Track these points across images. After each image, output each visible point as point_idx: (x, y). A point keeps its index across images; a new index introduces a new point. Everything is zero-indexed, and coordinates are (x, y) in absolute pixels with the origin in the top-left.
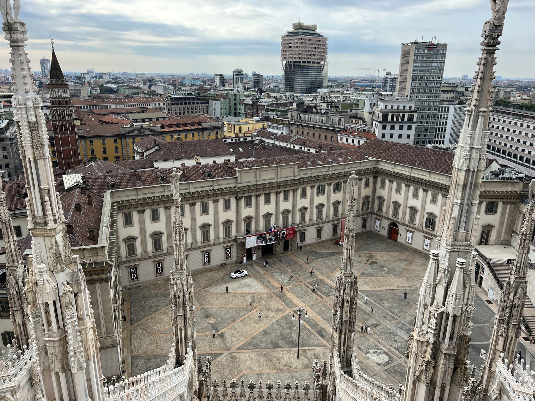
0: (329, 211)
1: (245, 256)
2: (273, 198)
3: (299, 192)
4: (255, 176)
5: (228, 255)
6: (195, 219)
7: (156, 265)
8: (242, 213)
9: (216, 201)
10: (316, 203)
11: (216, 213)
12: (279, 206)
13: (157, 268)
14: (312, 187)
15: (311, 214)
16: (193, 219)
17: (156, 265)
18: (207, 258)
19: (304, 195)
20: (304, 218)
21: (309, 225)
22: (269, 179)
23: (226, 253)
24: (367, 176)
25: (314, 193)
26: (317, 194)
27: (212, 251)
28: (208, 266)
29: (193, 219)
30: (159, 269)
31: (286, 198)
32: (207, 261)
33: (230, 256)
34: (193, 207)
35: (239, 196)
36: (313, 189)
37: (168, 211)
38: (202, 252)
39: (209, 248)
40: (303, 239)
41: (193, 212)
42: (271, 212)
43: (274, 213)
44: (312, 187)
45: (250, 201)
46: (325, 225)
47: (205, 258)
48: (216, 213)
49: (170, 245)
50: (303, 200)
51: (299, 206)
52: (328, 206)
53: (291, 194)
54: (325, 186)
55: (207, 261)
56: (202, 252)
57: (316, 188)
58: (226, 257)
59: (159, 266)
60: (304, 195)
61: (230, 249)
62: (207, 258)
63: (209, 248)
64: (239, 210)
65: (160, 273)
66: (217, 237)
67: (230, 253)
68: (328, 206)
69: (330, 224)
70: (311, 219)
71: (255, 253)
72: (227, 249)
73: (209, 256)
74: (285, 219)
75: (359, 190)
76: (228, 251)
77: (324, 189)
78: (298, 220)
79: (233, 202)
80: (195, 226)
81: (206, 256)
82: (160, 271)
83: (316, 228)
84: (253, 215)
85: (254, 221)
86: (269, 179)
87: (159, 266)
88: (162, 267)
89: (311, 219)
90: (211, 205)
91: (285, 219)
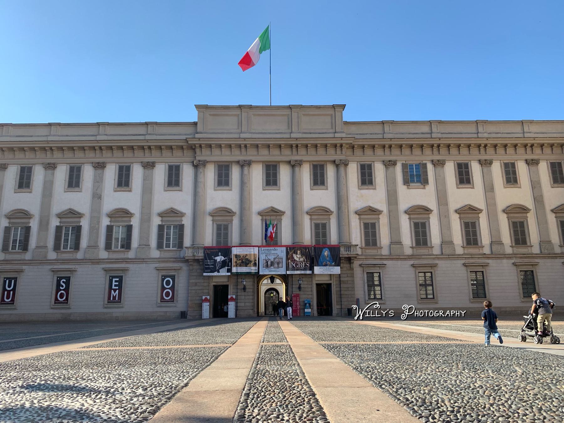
0: (449, 228)
1: (206, 300)
2: (284, 173)
4: (238, 126)
5: (168, 294)
6: (100, 197)
7: (5, 282)
8: (208, 201)
9: (149, 166)
11: (147, 190)
13: (4, 289)
15: (394, 228)
16: (97, 196)
17: (5, 282)
18: (115, 290)
21: (391, 257)
22: (270, 133)
23: (163, 288)
26: (406, 182)
28: (116, 311)
29: (97, 196)
30: (9, 292)
32: (114, 298)
34: (99, 171)
35: (198, 158)
36: (391, 169)
37: (50, 172)
41: (98, 181)
43: (288, 213)
44: (389, 164)
45: (227, 176)
46: (442, 264)
47: (110, 288)
48: (147, 190)
49: (42, 244)
50: (367, 192)
52: (444, 218)
54: (425, 166)
55: (114, 298)
57: (399, 168)
58: (162, 298)
59: (9, 287)
61: (173, 277)
62: (115, 290)
64: (200, 190)
65: (8, 303)
66: (145, 245)
67: (173, 288)
68: (444, 218)
71: (232, 299)
72: (165, 277)
73: (120, 286)
75: (533, 188)
76: (168, 283)
77: (426, 173)
79: (187, 172)
80: (99, 212)
81: (114, 283)
82: (8, 298)
83: (413, 266)
84: (234, 207)
85: (236, 221)
86: (270, 133)
87: (9, 287)
88: (14, 290)
89: (396, 242)
90: (137, 173)
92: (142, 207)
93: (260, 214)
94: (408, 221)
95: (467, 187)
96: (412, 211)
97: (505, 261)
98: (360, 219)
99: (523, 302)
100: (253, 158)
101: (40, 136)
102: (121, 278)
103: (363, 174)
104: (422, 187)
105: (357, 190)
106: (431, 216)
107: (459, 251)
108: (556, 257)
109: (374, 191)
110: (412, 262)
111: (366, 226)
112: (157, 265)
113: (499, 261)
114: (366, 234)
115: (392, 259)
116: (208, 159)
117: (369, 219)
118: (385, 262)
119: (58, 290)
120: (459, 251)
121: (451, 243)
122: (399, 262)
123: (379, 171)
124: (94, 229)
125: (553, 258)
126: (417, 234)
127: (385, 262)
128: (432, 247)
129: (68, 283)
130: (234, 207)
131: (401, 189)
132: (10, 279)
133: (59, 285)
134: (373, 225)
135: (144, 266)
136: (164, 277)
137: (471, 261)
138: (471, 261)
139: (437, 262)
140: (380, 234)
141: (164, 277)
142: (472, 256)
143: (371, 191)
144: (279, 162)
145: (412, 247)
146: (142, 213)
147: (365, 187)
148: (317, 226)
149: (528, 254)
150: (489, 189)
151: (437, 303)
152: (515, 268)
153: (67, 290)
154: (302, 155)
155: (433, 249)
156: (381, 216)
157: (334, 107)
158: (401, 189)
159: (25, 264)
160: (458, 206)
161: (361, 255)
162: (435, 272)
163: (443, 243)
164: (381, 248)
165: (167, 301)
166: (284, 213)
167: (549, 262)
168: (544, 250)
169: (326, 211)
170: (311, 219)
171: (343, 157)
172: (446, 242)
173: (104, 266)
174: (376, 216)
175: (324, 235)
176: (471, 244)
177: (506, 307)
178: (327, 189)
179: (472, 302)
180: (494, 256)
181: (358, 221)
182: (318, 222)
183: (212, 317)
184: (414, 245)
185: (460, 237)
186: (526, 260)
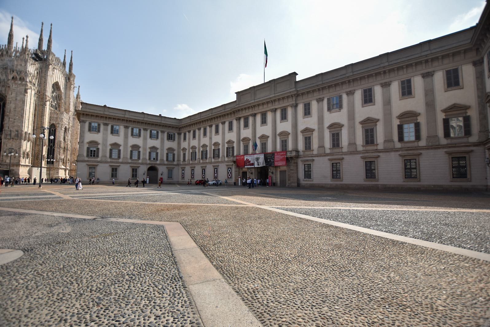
2: (269, 116)
3: (301, 108)
10: (327, 124)
12: (272, 126)
14: (320, 100)
15: (321, 138)
16: (211, 138)
19: (307, 112)
20: (310, 143)
21: (317, 156)
23: (228, 173)
24: (450, 65)
25: (322, 109)
26: (329, 109)
27: (219, 167)
29: (211, 138)
31: (284, 117)
33: (231, 177)
34: (211, 128)
35: (237, 116)
36: (321, 103)
38: (214, 166)
39: (217, 164)
40: (308, 175)
41: (211, 132)
42: (267, 134)
44: (320, 100)
48: (224, 134)
50: (308, 119)
51: (301, 127)
52: (352, 128)
53: (290, 111)
56: (214, 166)
57: (325, 102)
60: (307, 112)
63: (217, 164)
68: (352, 128)
69: (358, 157)
70: (321, 146)
74: (284, 143)
75: (426, 95)
78: (301, 146)
81: (216, 171)
83: (329, 160)
84: (250, 136)
89: (321, 146)
91: (284, 143)
92: (222, 141)
93: (259, 138)
94: (329, 133)
95: (369, 105)
96: (331, 127)
97: (393, 153)
98: (303, 135)
99: (404, 181)
100: (255, 112)
101: (198, 118)
102: (217, 169)
103: (305, 109)
104: (339, 111)
105: (302, 119)
106: (343, 128)
107: (360, 148)
108: (439, 148)
109: (311, 118)
110: (329, 157)
111: (306, 138)
112: (226, 164)
113: (388, 154)
114: (306, 143)
115: (318, 156)
116: (240, 116)
117: (307, 134)
118: (314, 158)
119: (203, 174)
120: (360, 148)
121: (355, 144)
122: (322, 158)
123: (314, 106)
124: (210, 151)
125: (435, 148)
126: (333, 140)
127: (314, 158)
128: (342, 148)
129: (204, 171)
130: (250, 137)
131: (326, 114)
132: (192, 170)
133: (203, 172)
134: (310, 138)
135: (223, 164)
136: (229, 168)
137: (366, 155)
138: (366, 155)
139: (343, 156)
140: (303, 143)
141: (229, 168)
142: (367, 151)
143: (309, 119)
144: (267, 111)
145: (330, 149)
146: (222, 143)
147: (306, 117)
148: (282, 141)
149: (412, 147)
150: (387, 102)
151: (342, 181)
152: (400, 158)
153: (204, 173)
154: (277, 105)
155: (343, 149)
156: (314, 132)
157: (290, 75)
158: (326, 114)
159: (195, 165)
160: (362, 119)
161: (303, 155)
162: (342, 162)
163: (350, 144)
164: (313, 150)
165: (229, 178)
166: (268, 137)
167: (431, 152)
168: (429, 143)
169: (311, 131)
170: (260, 141)
171: (294, 102)
172: (352, 144)
173: (213, 165)
174: (311, 133)
175: (286, 146)
176: (335, 147)
177: (391, 185)
178: (288, 121)
179: (365, 181)
180: (386, 151)
181: (302, 136)
182: (283, 139)
183: (241, 184)
184: (331, 147)
185: (361, 140)
186: (410, 152)
